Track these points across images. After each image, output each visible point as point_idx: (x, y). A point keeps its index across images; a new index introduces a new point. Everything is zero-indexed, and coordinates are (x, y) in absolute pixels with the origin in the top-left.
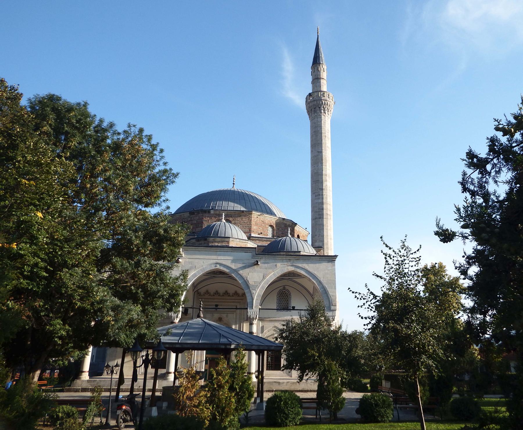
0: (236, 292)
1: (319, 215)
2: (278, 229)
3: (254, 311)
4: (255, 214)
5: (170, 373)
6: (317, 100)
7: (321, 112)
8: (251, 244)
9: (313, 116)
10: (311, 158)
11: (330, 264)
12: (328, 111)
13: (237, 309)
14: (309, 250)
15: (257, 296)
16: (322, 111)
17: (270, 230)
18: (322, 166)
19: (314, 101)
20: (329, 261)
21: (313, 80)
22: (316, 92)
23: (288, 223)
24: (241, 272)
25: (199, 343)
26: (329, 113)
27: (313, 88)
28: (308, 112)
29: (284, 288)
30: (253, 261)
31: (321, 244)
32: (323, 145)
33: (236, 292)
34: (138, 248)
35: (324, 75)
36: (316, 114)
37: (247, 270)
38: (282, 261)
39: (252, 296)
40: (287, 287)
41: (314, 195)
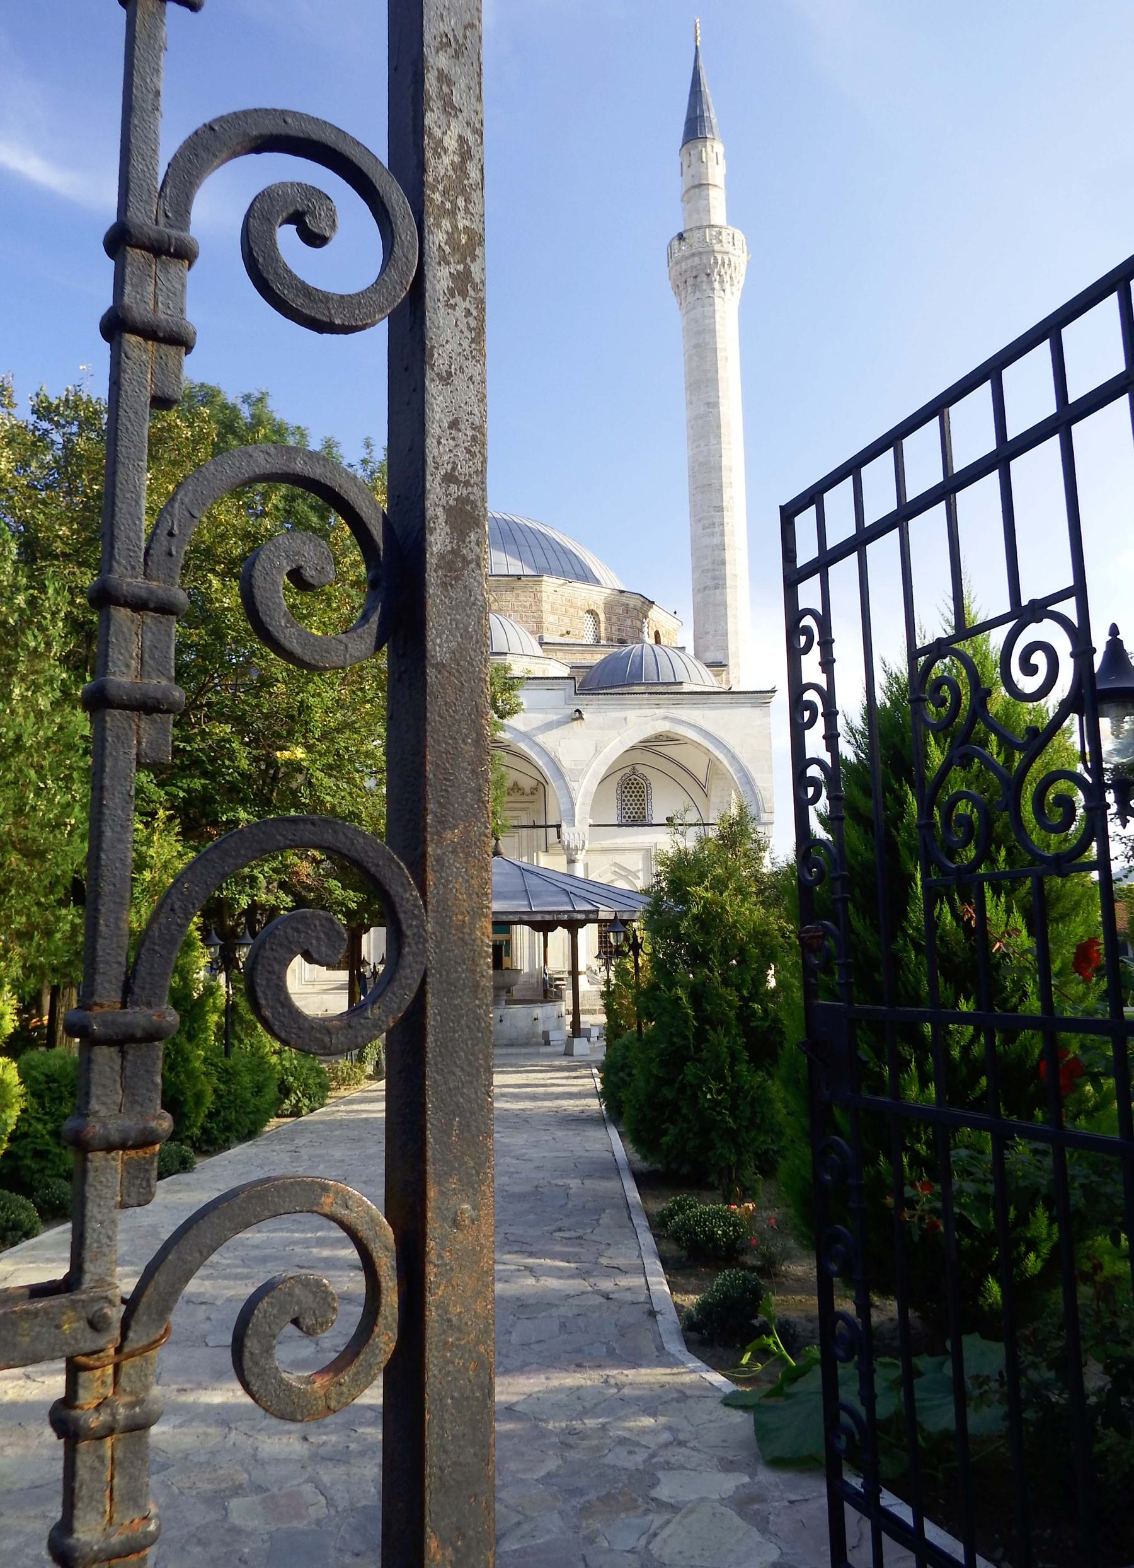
0: (516, 784)
1: (714, 578)
2: (608, 619)
7: (713, 289)
8: (557, 669)
9: (691, 298)
11: (757, 712)
12: (732, 285)
13: (534, 827)
14: (701, 679)
16: (717, 285)
17: (589, 621)
18: (720, 443)
19: (693, 255)
20: (754, 705)
21: (687, 192)
22: (699, 228)
24: (540, 739)
26: (735, 289)
31: (718, 657)
33: (516, 784)
35: (717, 173)
36: (698, 295)
37: (555, 733)
38: (641, 706)
39: (570, 797)
41: (700, 525)
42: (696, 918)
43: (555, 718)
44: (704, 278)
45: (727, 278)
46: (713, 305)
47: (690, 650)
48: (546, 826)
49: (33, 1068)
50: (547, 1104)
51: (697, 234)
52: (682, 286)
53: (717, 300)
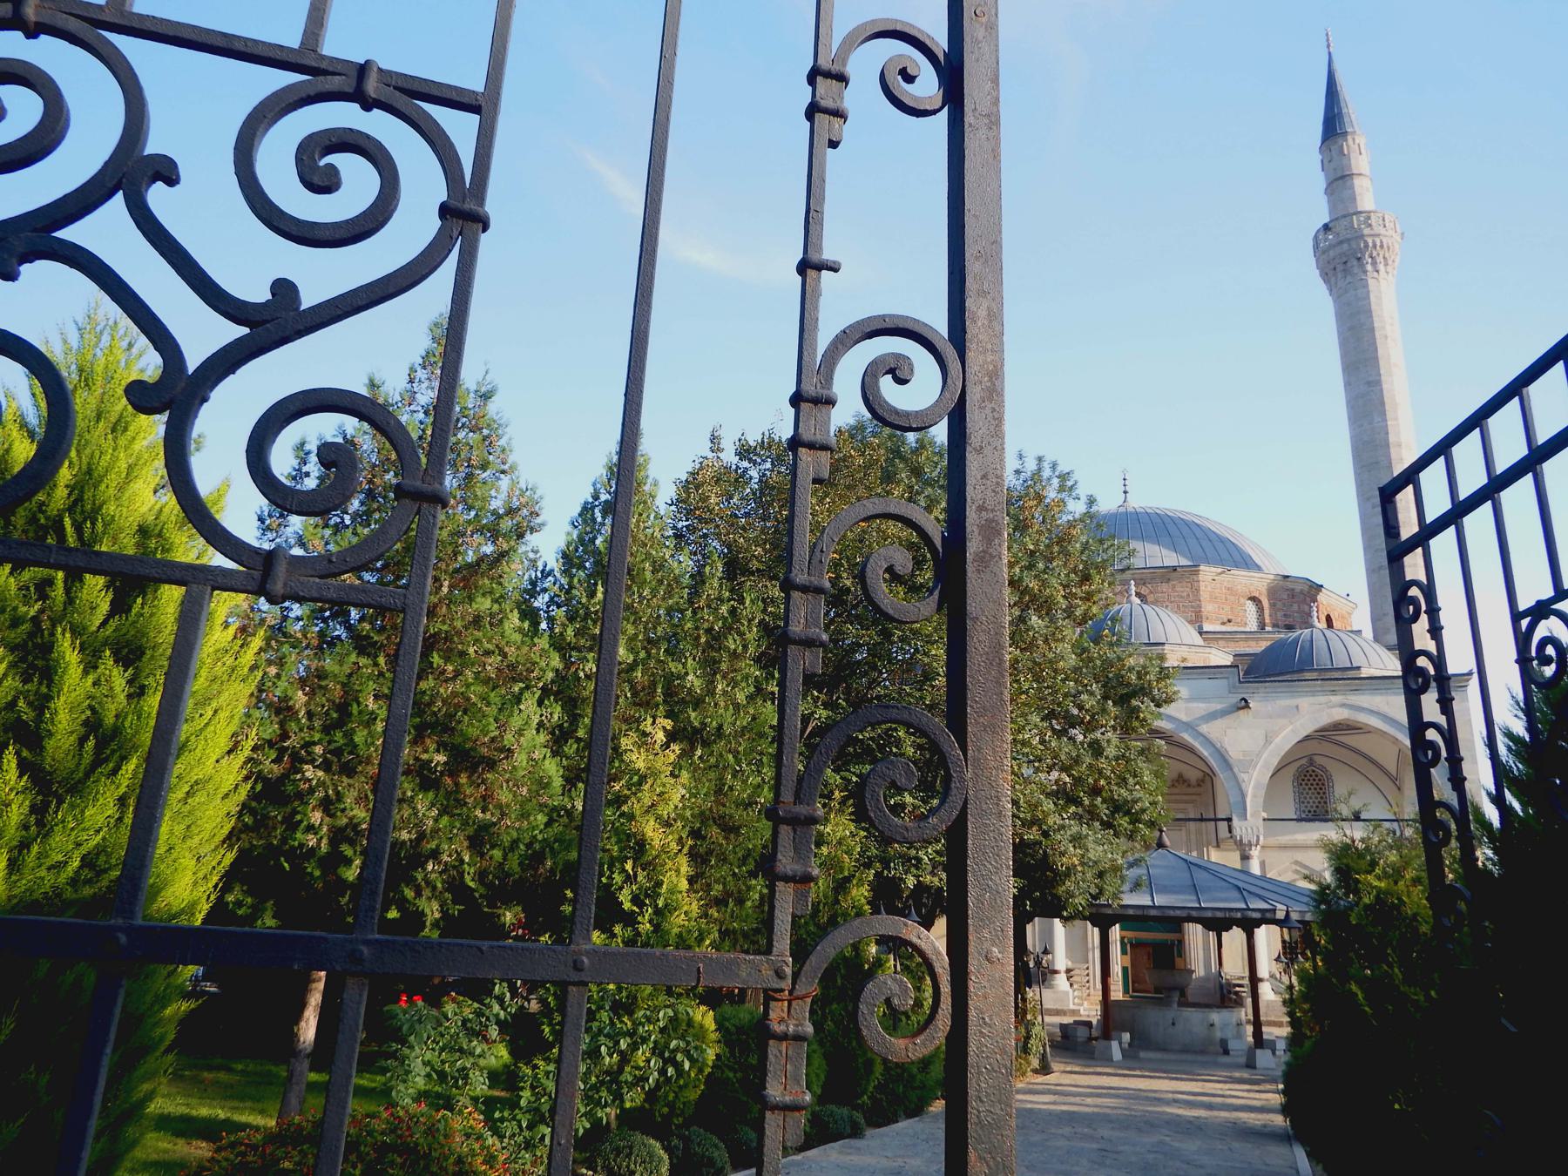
0: (1180, 776)
2: (1273, 606)
3: (1249, 826)
4: (1207, 572)
5: (1056, 972)
6: (1348, 240)
7: (1365, 272)
8: (1220, 657)
10: (1348, 402)
13: (1202, 820)
15: (1256, 787)
16: (1369, 267)
17: (1251, 608)
19: (1341, 242)
23: (1298, 588)
24: (1204, 728)
25: (1201, 908)
27: (1333, 206)
28: (1325, 276)
29: (1311, 762)
30: (1235, 698)
32: (1381, 363)
33: (1180, 776)
34: (1092, 717)
36: (1349, 279)
38: (1314, 693)
40: (1319, 760)
42: (1367, 907)
43: (1219, 707)
44: (1355, 262)
45: (1380, 259)
46: (1366, 286)
47: (1368, 633)
48: (1216, 820)
49: (728, 1020)
50: (1224, 1114)
51: (1344, 222)
52: (1331, 273)
53: (1371, 282)
